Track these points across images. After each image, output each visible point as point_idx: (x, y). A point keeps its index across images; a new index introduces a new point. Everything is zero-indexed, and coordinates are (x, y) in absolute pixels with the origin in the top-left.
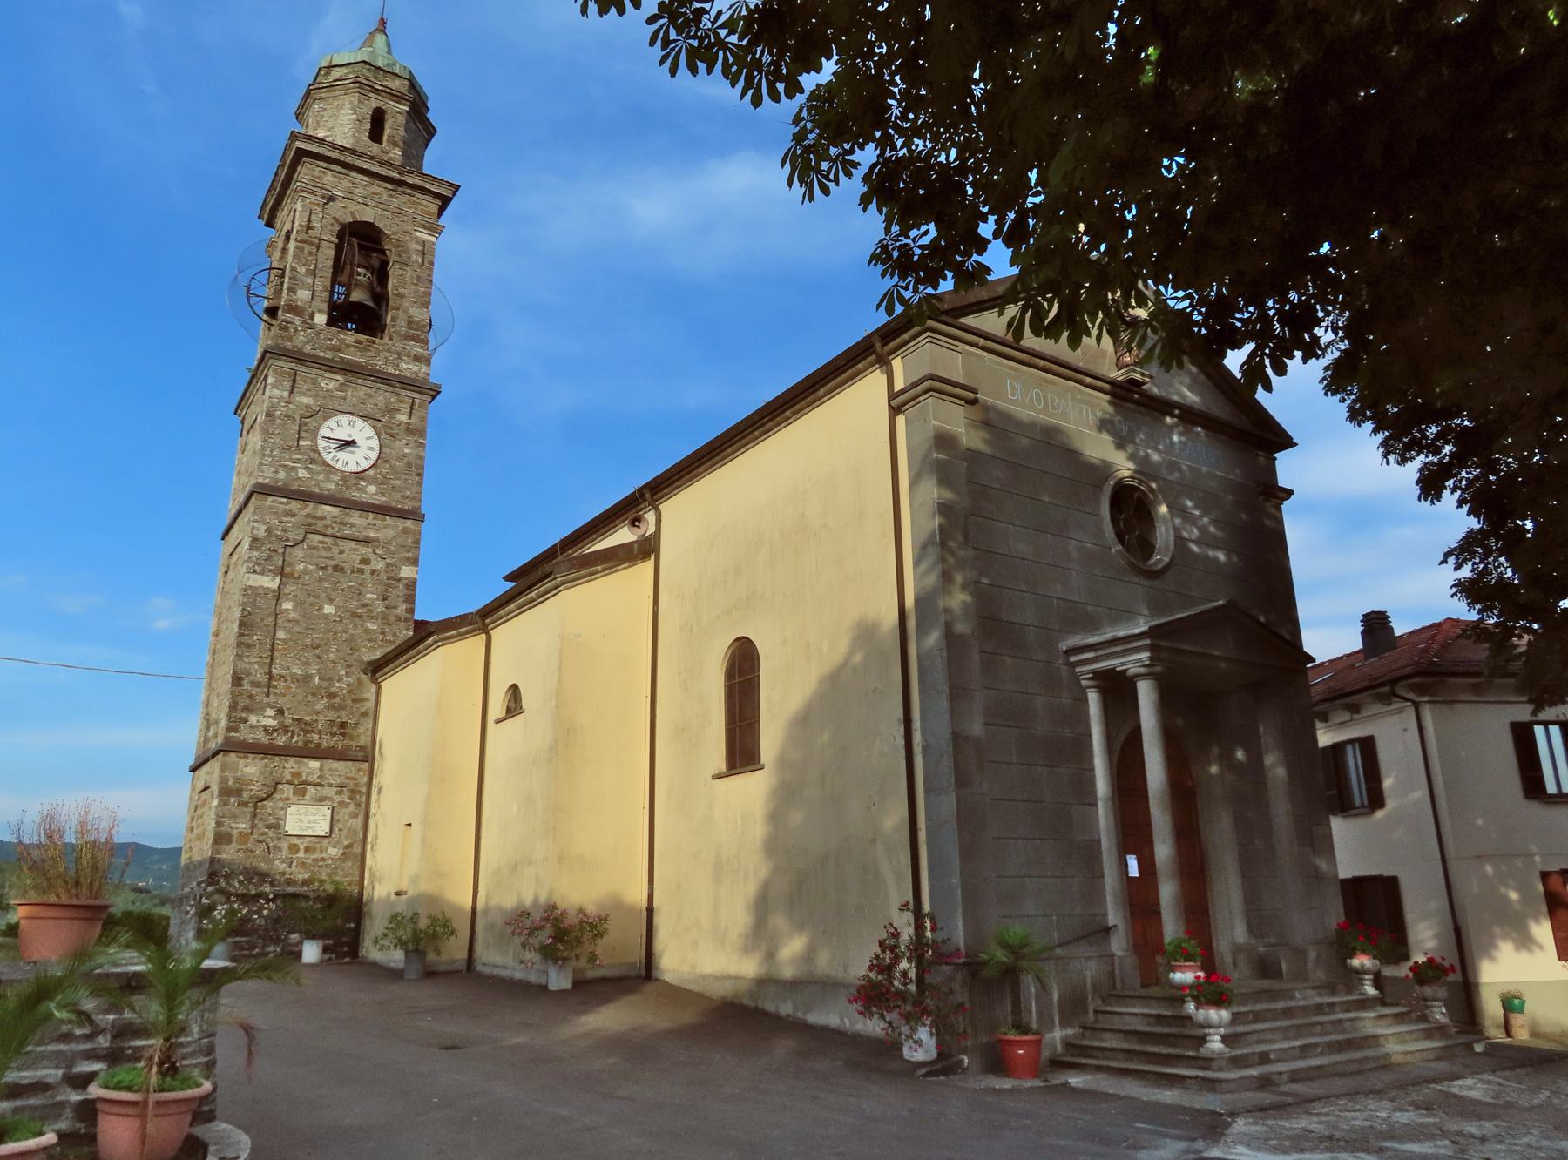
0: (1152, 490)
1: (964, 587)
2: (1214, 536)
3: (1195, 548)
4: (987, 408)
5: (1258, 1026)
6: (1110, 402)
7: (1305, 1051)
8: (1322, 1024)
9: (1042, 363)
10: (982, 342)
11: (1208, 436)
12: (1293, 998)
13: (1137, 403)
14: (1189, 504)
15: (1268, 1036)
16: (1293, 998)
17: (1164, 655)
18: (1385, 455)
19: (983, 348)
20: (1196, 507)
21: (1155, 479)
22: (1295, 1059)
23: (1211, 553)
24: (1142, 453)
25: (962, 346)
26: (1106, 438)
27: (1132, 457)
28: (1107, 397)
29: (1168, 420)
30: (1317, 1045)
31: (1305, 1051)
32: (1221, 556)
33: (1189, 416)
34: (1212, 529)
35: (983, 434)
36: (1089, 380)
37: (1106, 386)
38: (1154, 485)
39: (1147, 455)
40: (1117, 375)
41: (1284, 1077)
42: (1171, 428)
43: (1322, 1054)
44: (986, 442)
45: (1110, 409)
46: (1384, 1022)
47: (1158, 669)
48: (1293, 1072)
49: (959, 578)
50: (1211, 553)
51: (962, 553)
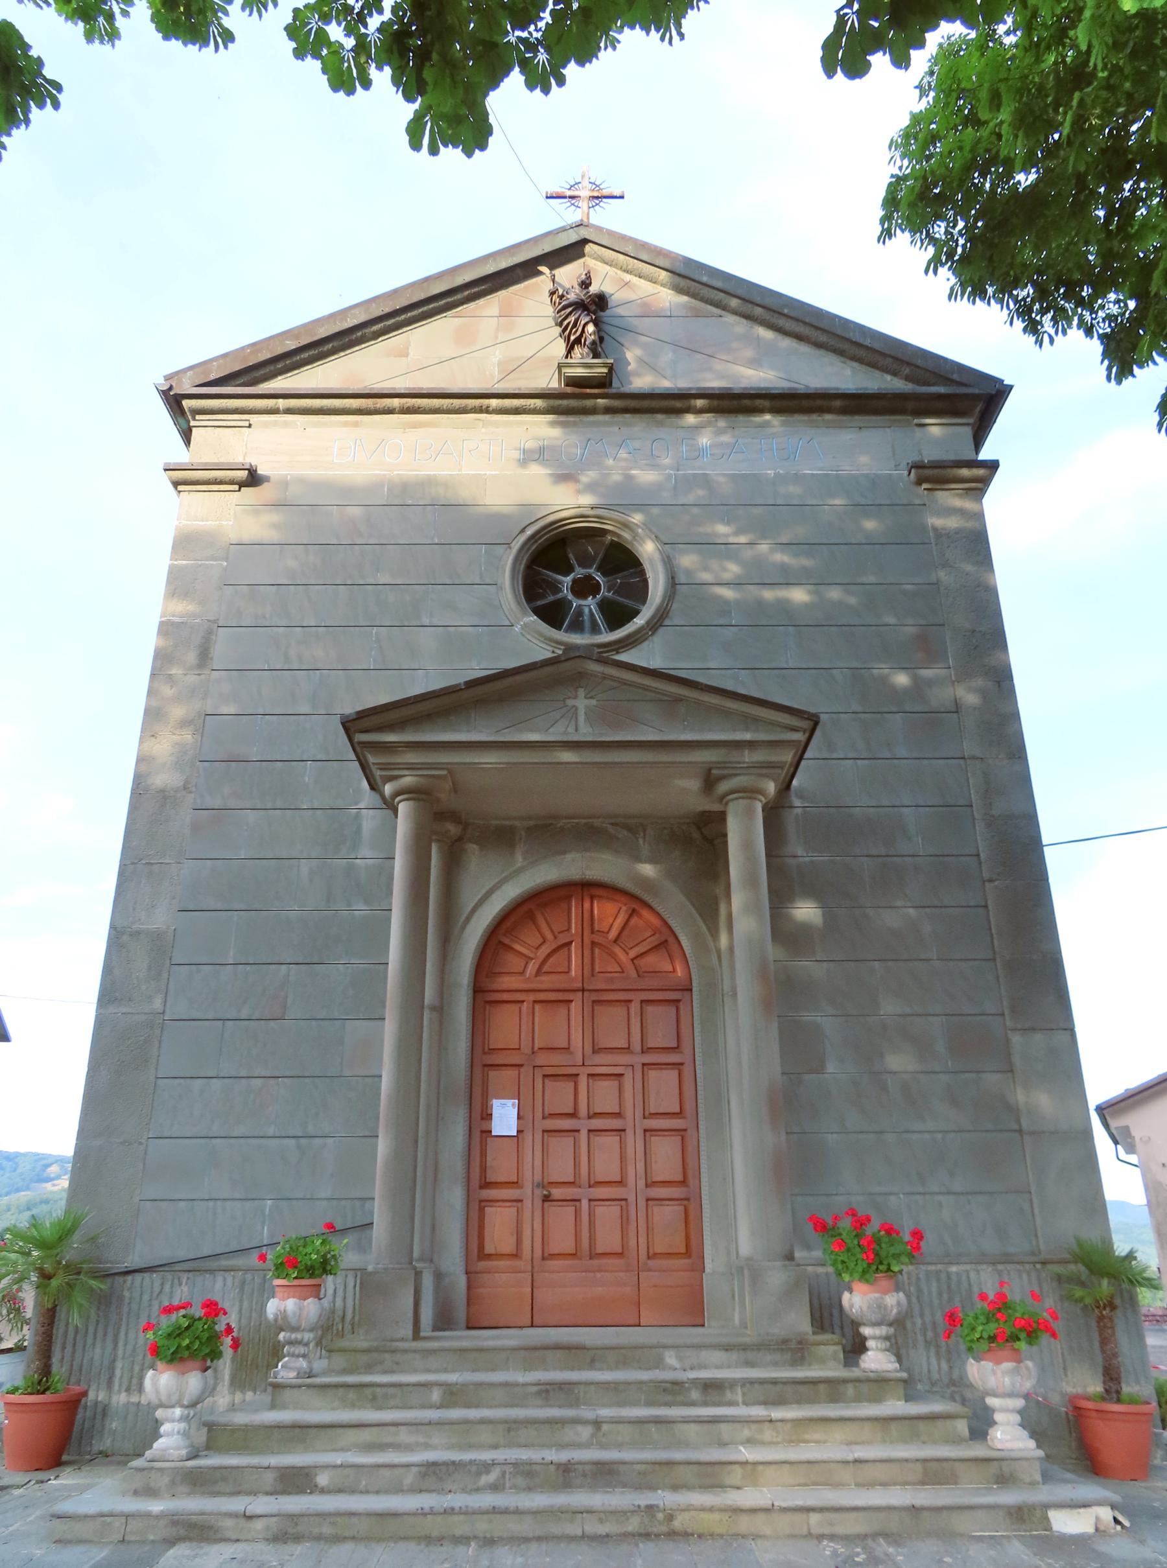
0: (626, 526)
1: (183, 723)
2: (784, 568)
3: (727, 593)
4: (285, 484)
5: (455, 1414)
6: (553, 424)
7: (434, 1474)
8: (597, 1424)
9: (396, 402)
10: (282, 403)
11: (783, 424)
12: (659, 1364)
13: (608, 410)
14: (722, 529)
15: (404, 1436)
16: (659, 1364)
17: (411, 758)
18: (1033, 328)
19: (289, 411)
20: (737, 533)
21: (639, 507)
22: (398, 1489)
23: (768, 594)
24: (616, 477)
25: (254, 418)
26: (537, 470)
27: (591, 488)
28: (550, 417)
29: (690, 419)
30: (487, 1467)
31: (434, 1474)
32: (799, 595)
33: (733, 404)
34: (780, 557)
35: (274, 517)
36: (494, 403)
37: (538, 403)
38: (637, 518)
39: (629, 478)
40: (551, 381)
41: (259, 1525)
42: (697, 428)
43: (496, 1487)
44: (276, 526)
45: (556, 432)
46: (839, 1433)
47: (408, 780)
48: (293, 1518)
49: (178, 712)
50: (768, 594)
51: (192, 679)
